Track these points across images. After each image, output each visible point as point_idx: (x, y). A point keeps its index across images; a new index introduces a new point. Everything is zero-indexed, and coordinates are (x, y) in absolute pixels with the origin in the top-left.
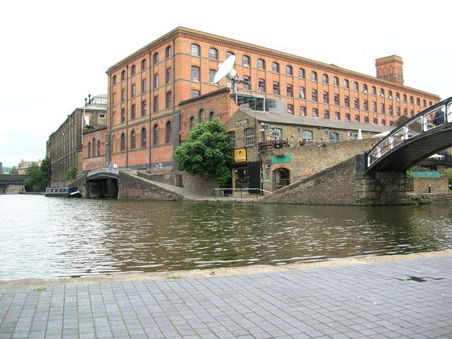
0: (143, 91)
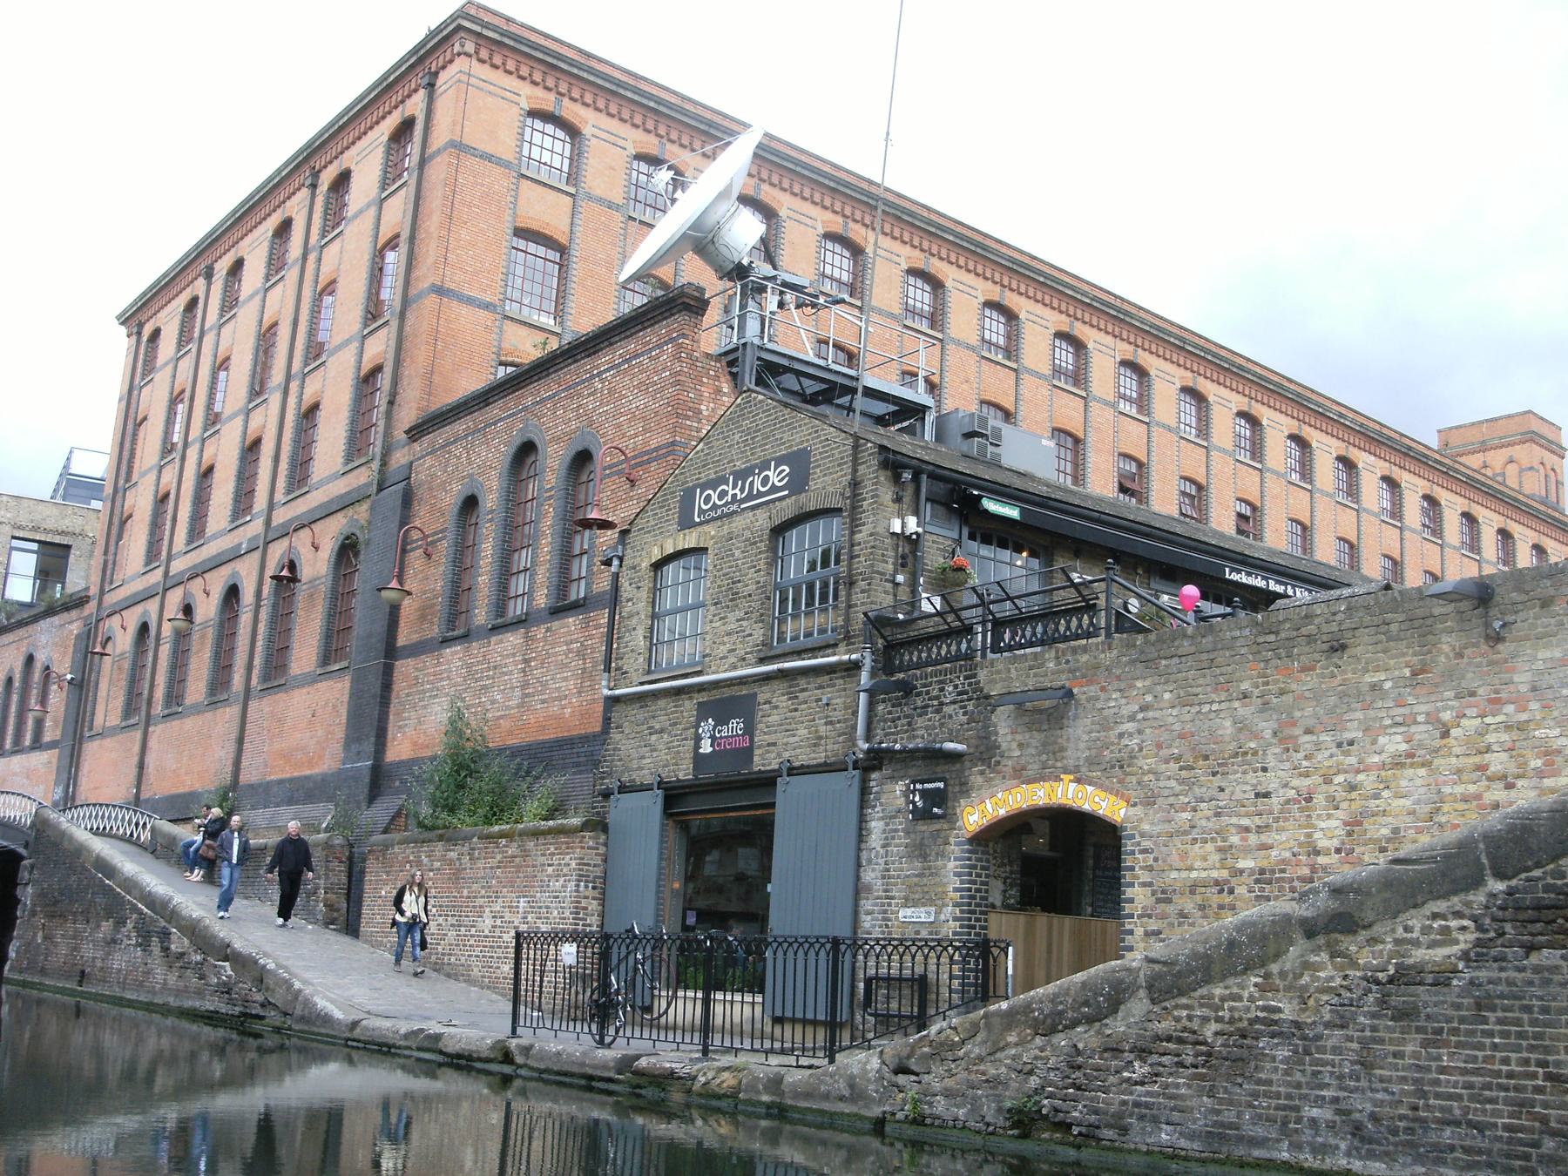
0: (257, 390)
